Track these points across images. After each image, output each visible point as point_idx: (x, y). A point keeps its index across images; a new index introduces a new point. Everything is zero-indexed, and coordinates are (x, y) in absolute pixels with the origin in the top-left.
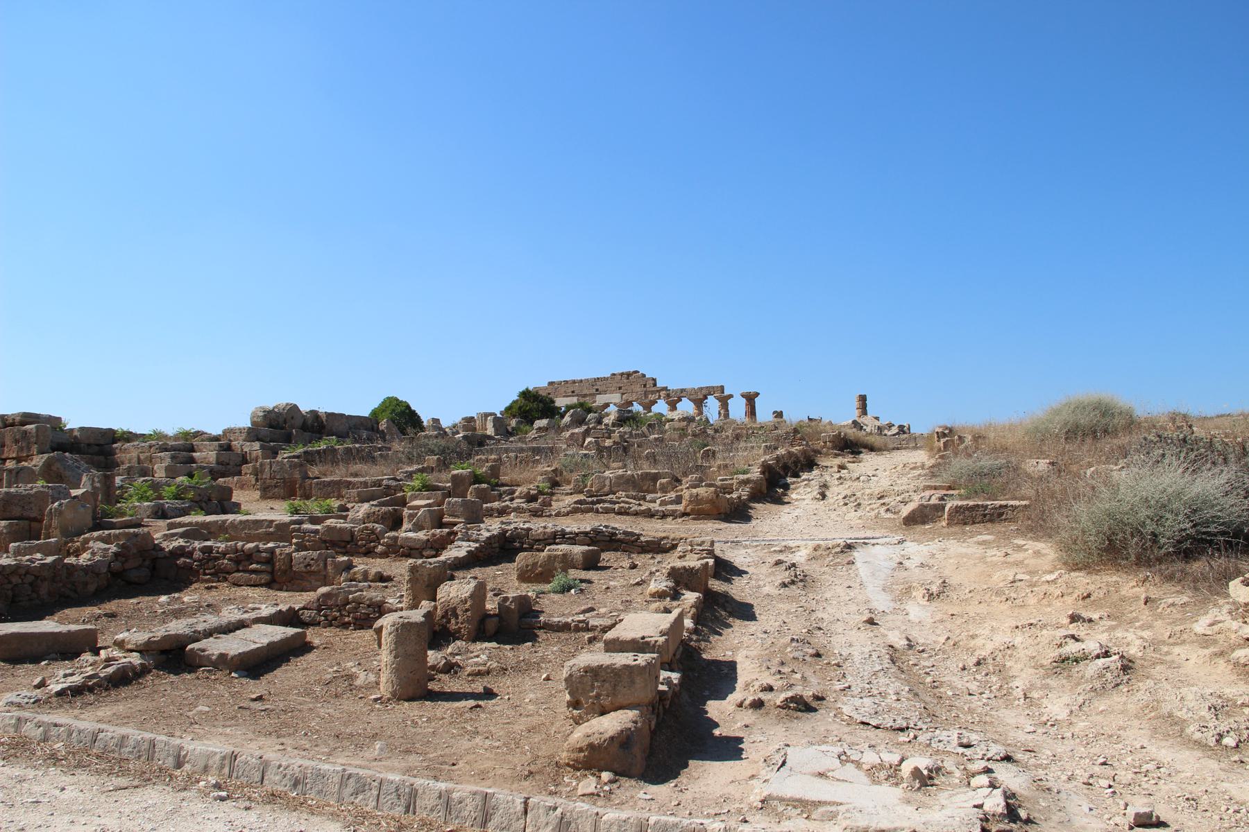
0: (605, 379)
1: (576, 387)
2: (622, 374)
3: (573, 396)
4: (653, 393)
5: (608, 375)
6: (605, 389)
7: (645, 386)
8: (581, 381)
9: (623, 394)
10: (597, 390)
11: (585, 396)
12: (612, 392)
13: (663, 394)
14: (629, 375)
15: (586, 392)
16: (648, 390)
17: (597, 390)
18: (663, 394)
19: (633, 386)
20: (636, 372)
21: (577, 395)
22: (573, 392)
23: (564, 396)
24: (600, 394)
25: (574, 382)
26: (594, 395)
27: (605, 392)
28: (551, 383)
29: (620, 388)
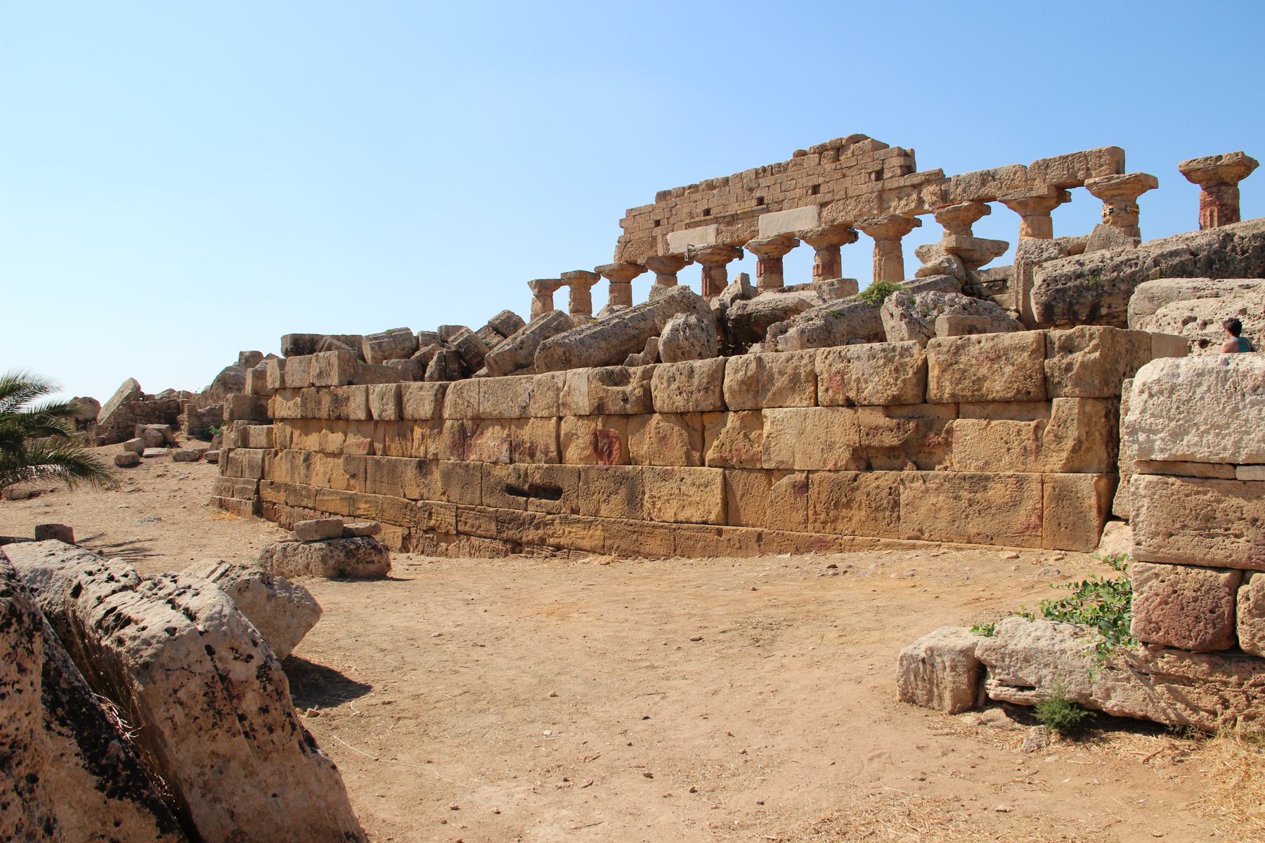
0: (781, 168)
1: (713, 201)
2: (821, 150)
3: (706, 223)
4: (900, 192)
5: (786, 157)
6: (776, 193)
7: (879, 175)
8: (726, 181)
9: (823, 205)
10: (761, 201)
11: (733, 219)
12: (796, 203)
13: (928, 193)
14: (838, 149)
15: (735, 208)
16: (888, 185)
17: (761, 201)
18: (928, 193)
20: (856, 139)
21: (717, 220)
22: (707, 212)
23: (688, 226)
24: (768, 210)
25: (711, 186)
26: (751, 215)
27: (779, 205)
28: (663, 196)
29: (816, 190)
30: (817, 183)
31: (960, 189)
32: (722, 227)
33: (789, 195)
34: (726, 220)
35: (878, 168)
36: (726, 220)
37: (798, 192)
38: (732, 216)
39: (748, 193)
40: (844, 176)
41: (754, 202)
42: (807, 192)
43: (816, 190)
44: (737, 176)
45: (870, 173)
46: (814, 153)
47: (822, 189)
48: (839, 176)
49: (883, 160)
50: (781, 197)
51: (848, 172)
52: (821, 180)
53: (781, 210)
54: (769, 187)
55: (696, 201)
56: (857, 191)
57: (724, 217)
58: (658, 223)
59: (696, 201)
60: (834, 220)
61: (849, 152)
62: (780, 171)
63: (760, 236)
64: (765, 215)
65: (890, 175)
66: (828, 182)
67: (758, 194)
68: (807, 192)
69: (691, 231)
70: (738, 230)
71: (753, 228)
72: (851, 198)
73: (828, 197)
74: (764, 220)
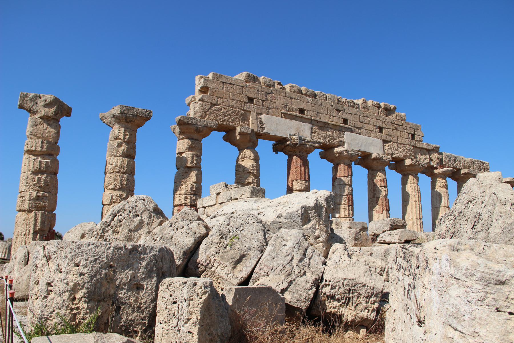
9: (385, 142)
12: (369, 133)
17: (345, 121)
19: (398, 133)
22: (302, 111)
23: (285, 116)
30: (381, 126)
31: (447, 160)
32: (315, 128)
33: (365, 126)
34: (319, 124)
35: (413, 133)
36: (319, 124)
37: (371, 127)
38: (325, 123)
39: (336, 112)
40: (396, 129)
41: (341, 121)
42: (376, 129)
43: (381, 129)
44: (323, 95)
45: (409, 134)
46: (375, 106)
47: (384, 131)
48: (394, 128)
49: (415, 129)
50: (360, 125)
51: (398, 128)
52: (383, 125)
53: (360, 134)
54: (352, 114)
55: (291, 98)
56: (403, 141)
57: (318, 122)
58: (251, 100)
59: (291, 98)
60: (392, 154)
61: (394, 115)
62: (354, 107)
63: (346, 147)
64: (349, 133)
65: (418, 139)
66: (387, 128)
67: (344, 116)
68: (376, 129)
69: (288, 121)
70: (329, 136)
71: (340, 139)
72: (401, 144)
73: (388, 138)
74: (347, 136)
